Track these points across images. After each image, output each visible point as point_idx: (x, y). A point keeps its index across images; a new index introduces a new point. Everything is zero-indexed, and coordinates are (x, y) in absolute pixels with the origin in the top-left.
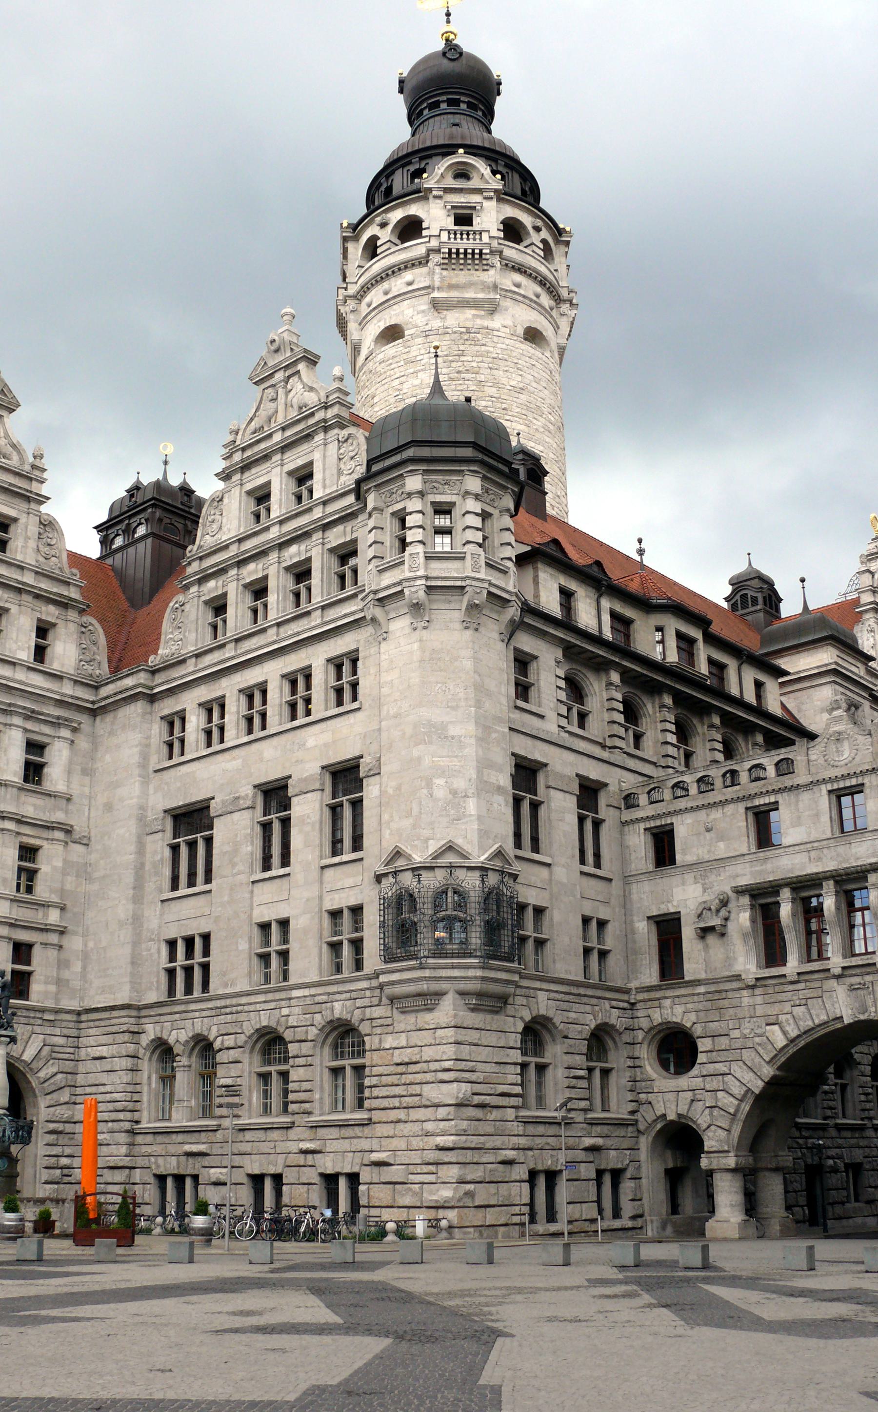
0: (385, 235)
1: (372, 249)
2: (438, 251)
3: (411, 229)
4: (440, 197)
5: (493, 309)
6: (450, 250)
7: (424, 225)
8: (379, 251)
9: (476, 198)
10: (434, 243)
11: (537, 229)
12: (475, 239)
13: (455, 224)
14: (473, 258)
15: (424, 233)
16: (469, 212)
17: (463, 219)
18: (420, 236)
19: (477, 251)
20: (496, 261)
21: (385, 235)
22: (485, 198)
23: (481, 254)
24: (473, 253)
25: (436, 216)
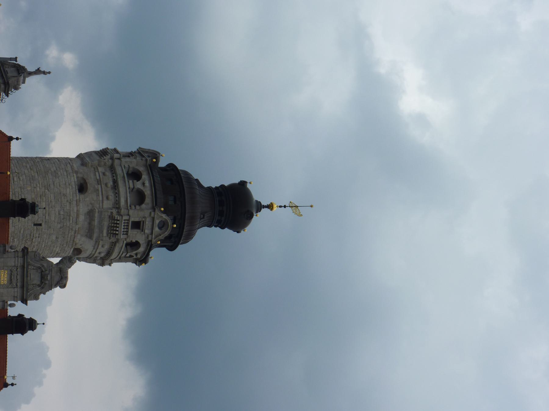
0: (138, 185)
1: (135, 175)
2: (119, 213)
6: (119, 220)
7: (138, 207)
8: (131, 181)
9: (147, 231)
11: (136, 254)
12: (124, 231)
15: (133, 207)
16: (141, 228)
17: (137, 225)
20: (113, 240)
21: (138, 185)
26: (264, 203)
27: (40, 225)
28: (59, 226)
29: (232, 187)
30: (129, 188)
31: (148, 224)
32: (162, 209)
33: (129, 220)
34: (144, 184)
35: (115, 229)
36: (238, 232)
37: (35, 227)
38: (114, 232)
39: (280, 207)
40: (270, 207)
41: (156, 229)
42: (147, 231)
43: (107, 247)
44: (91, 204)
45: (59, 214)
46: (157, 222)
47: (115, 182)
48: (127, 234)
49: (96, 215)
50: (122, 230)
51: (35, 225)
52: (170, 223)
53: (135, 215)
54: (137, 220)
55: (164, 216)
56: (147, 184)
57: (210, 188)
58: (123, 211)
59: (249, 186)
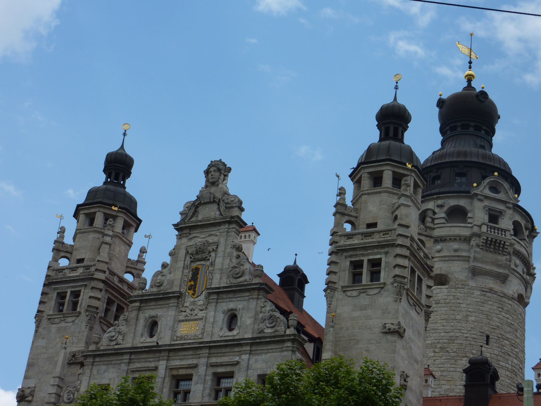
2: (478, 236)
3: (458, 214)
4: (481, 200)
5: (504, 279)
6: (488, 238)
7: (469, 215)
9: (501, 207)
10: (476, 229)
13: (490, 221)
14: (499, 247)
15: (469, 220)
16: (497, 214)
17: (494, 217)
18: (465, 221)
19: (502, 242)
22: (508, 208)
23: (504, 245)
24: (500, 243)
25: (478, 214)
26: (466, 84)
27: (488, 337)
30: (444, 223)
32: (475, 185)
33: (488, 226)
34: (441, 206)
36: (499, 118)
39: (470, 67)
40: (470, 79)
41: (501, 196)
42: (501, 207)
43: (518, 262)
48: (505, 231)
51: (487, 344)
54: (486, 218)
56: (440, 202)
57: (443, 143)
59: (445, 97)
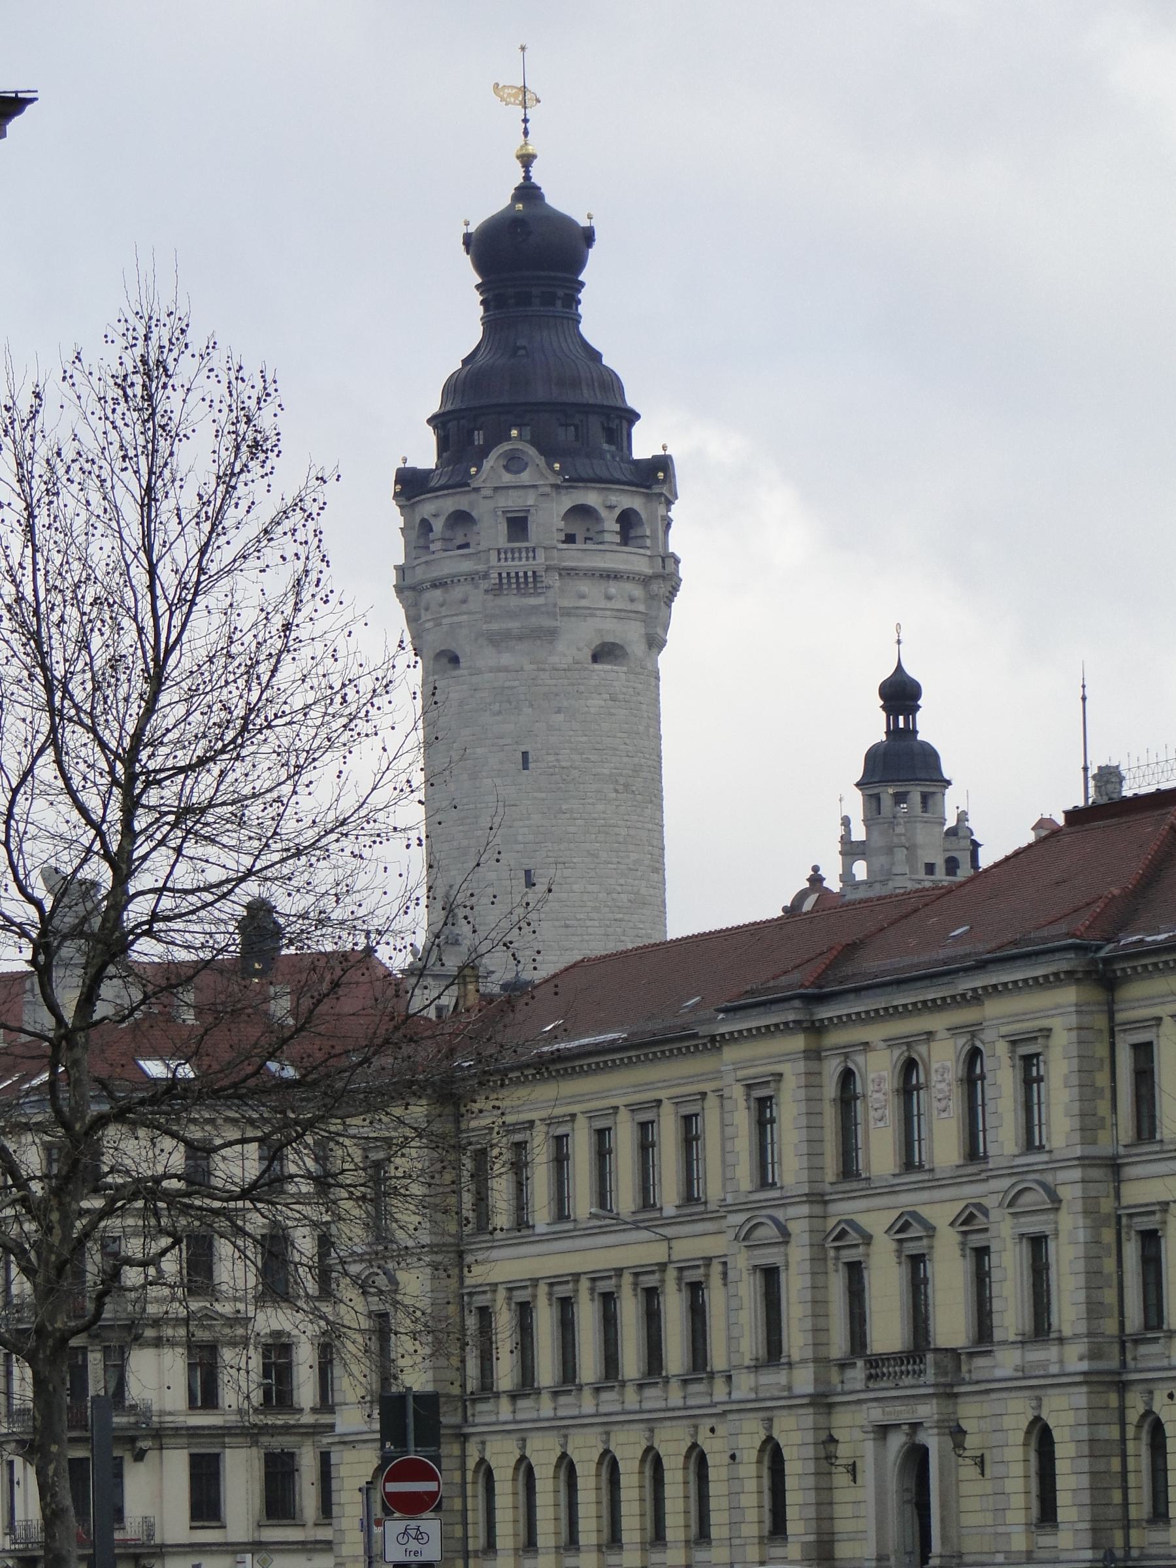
0: (438, 525)
5: (550, 635)
6: (500, 574)
9: (530, 499)
12: (527, 558)
17: (518, 525)
21: (438, 525)
27: (525, 755)
28: (527, 710)
29: (481, 265)
31: (512, 501)
35: (522, 580)
37: (531, 765)
38: (530, 580)
39: (526, 133)
40: (527, 160)
41: (525, 477)
42: (530, 499)
43: (585, 587)
44: (476, 639)
45: (499, 713)
46: (507, 478)
47: (437, 584)
49: (495, 626)
50: (524, 562)
51: (525, 767)
52: (505, 447)
53: (492, 533)
54: (503, 527)
55: (488, 464)
58: (481, 567)
59: (472, 229)
